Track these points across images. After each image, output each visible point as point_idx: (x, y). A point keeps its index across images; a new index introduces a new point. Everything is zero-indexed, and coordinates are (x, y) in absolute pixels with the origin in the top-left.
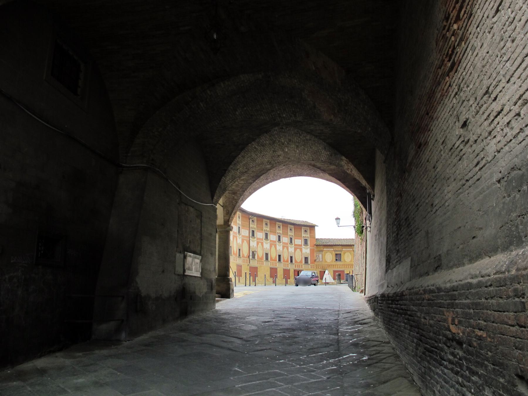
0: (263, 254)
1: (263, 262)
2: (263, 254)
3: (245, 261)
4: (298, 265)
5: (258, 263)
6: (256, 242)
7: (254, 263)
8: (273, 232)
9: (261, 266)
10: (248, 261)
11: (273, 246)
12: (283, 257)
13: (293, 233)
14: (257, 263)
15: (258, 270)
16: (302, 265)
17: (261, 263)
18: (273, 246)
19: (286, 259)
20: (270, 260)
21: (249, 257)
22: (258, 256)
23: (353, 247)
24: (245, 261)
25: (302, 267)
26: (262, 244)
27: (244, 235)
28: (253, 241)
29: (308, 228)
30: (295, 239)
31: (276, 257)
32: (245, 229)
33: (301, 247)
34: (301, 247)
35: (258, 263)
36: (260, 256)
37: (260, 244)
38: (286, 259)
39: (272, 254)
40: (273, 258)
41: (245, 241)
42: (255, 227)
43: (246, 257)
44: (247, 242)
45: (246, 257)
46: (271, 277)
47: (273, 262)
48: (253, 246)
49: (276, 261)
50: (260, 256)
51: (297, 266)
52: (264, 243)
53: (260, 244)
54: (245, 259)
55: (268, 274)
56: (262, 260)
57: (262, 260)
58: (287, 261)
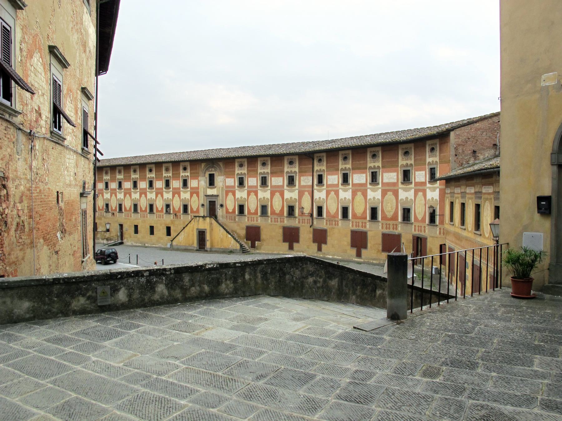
0: (338, 209)
1: (338, 221)
2: (338, 209)
3: (306, 221)
4: (418, 226)
5: (328, 223)
6: (324, 192)
7: (320, 224)
8: (359, 169)
9: (334, 228)
10: (311, 220)
11: (359, 194)
12: (383, 211)
13: (438, 157)
14: (327, 224)
15: (328, 234)
16: (425, 227)
17: (334, 223)
18: (359, 194)
19: (390, 215)
20: (352, 218)
21: (312, 215)
22: (328, 212)
23: (494, 178)
24: (306, 221)
25: (425, 231)
26: (337, 193)
27: (305, 184)
28: (319, 191)
29: (412, 145)
30: (416, 170)
31: (365, 212)
32: (308, 176)
33: (424, 188)
34: (424, 188)
35: (328, 223)
36: (333, 210)
37: (333, 193)
38: (392, 213)
39: (355, 208)
40: (359, 215)
41: (306, 193)
42: (324, 168)
43: (307, 216)
44: (309, 194)
45: (307, 216)
46: (353, 246)
47: (358, 220)
48: (320, 198)
49: (366, 218)
50: (333, 210)
51: (417, 228)
52: (340, 191)
53: (333, 193)
54: (306, 218)
55: (347, 240)
56: (336, 219)
57: (336, 219)
58: (395, 218)
